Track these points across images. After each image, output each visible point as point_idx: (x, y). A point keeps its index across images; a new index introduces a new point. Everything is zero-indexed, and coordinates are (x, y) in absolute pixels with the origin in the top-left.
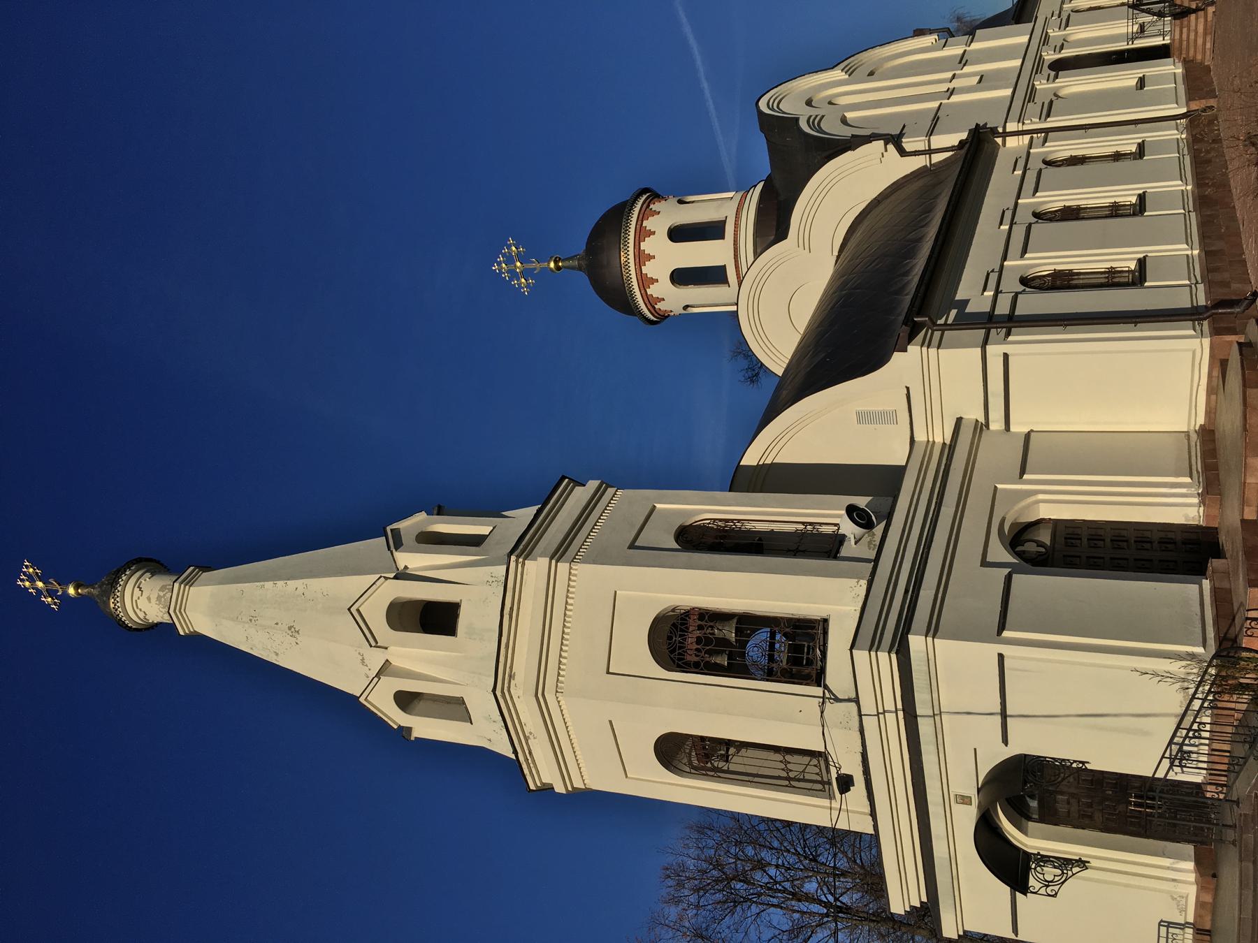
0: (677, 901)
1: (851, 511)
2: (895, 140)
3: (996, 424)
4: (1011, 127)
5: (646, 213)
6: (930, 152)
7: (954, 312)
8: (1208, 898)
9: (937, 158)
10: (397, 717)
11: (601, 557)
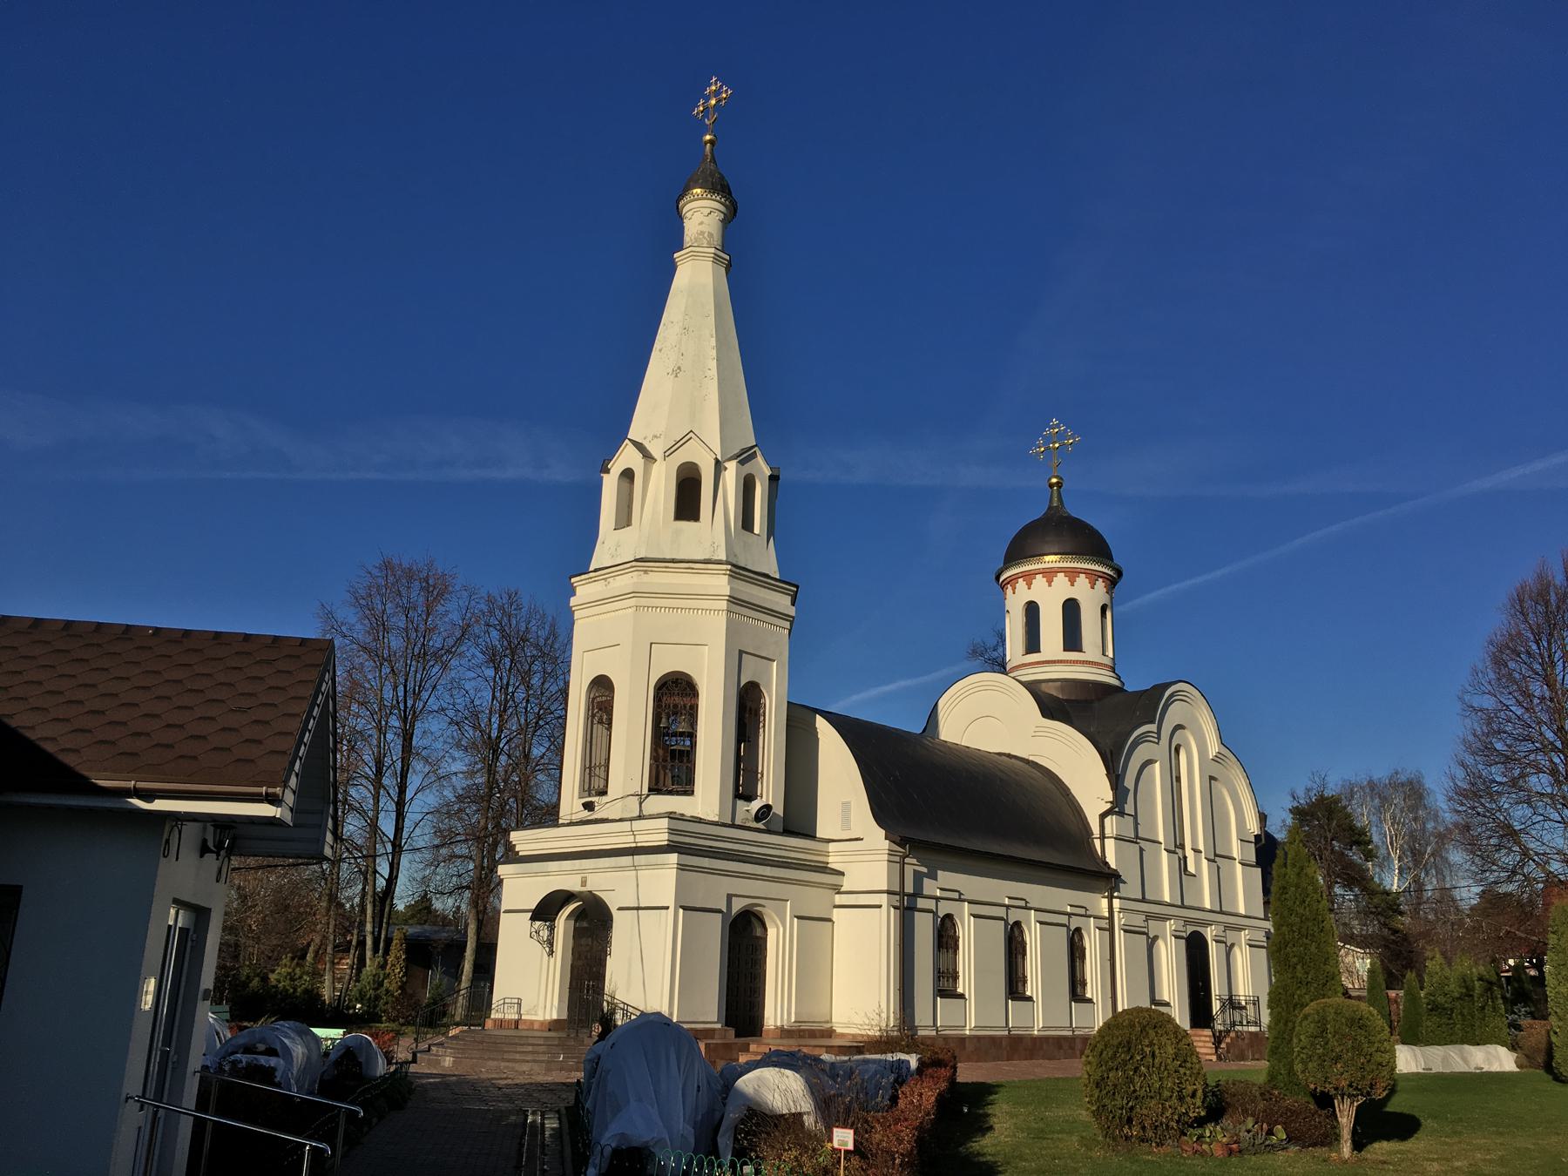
0: (492, 612)
1: (768, 807)
2: (1117, 808)
3: (839, 899)
4: (1116, 903)
5: (1093, 577)
6: (1103, 837)
8: (536, 1026)
9: (1097, 843)
10: (617, 466)
11: (732, 631)
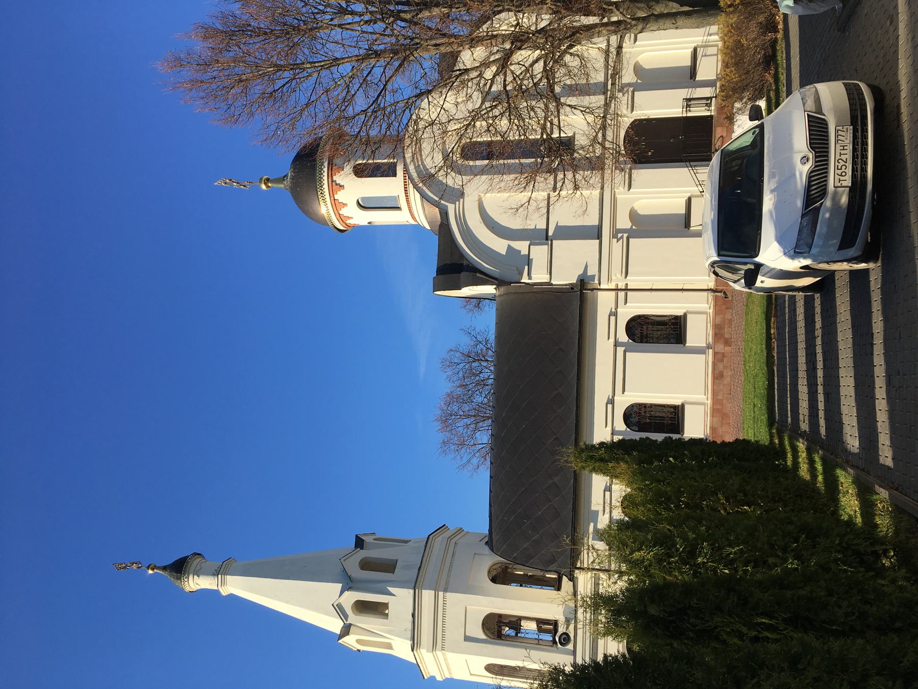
4: (602, 287)
5: (336, 187)
7: (592, 525)
